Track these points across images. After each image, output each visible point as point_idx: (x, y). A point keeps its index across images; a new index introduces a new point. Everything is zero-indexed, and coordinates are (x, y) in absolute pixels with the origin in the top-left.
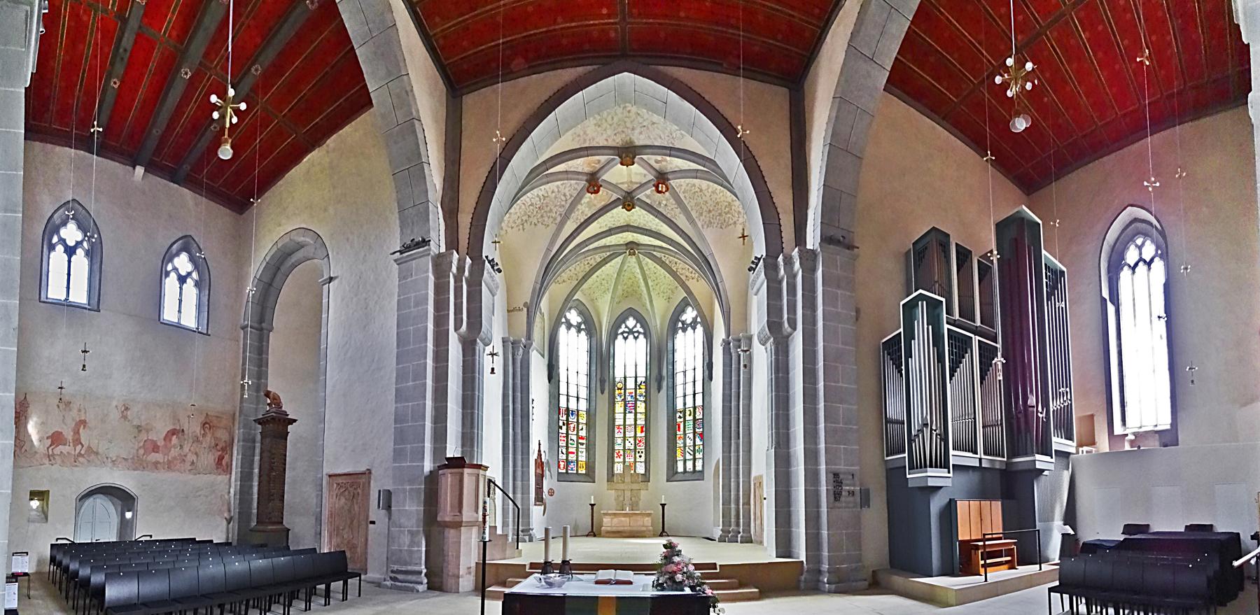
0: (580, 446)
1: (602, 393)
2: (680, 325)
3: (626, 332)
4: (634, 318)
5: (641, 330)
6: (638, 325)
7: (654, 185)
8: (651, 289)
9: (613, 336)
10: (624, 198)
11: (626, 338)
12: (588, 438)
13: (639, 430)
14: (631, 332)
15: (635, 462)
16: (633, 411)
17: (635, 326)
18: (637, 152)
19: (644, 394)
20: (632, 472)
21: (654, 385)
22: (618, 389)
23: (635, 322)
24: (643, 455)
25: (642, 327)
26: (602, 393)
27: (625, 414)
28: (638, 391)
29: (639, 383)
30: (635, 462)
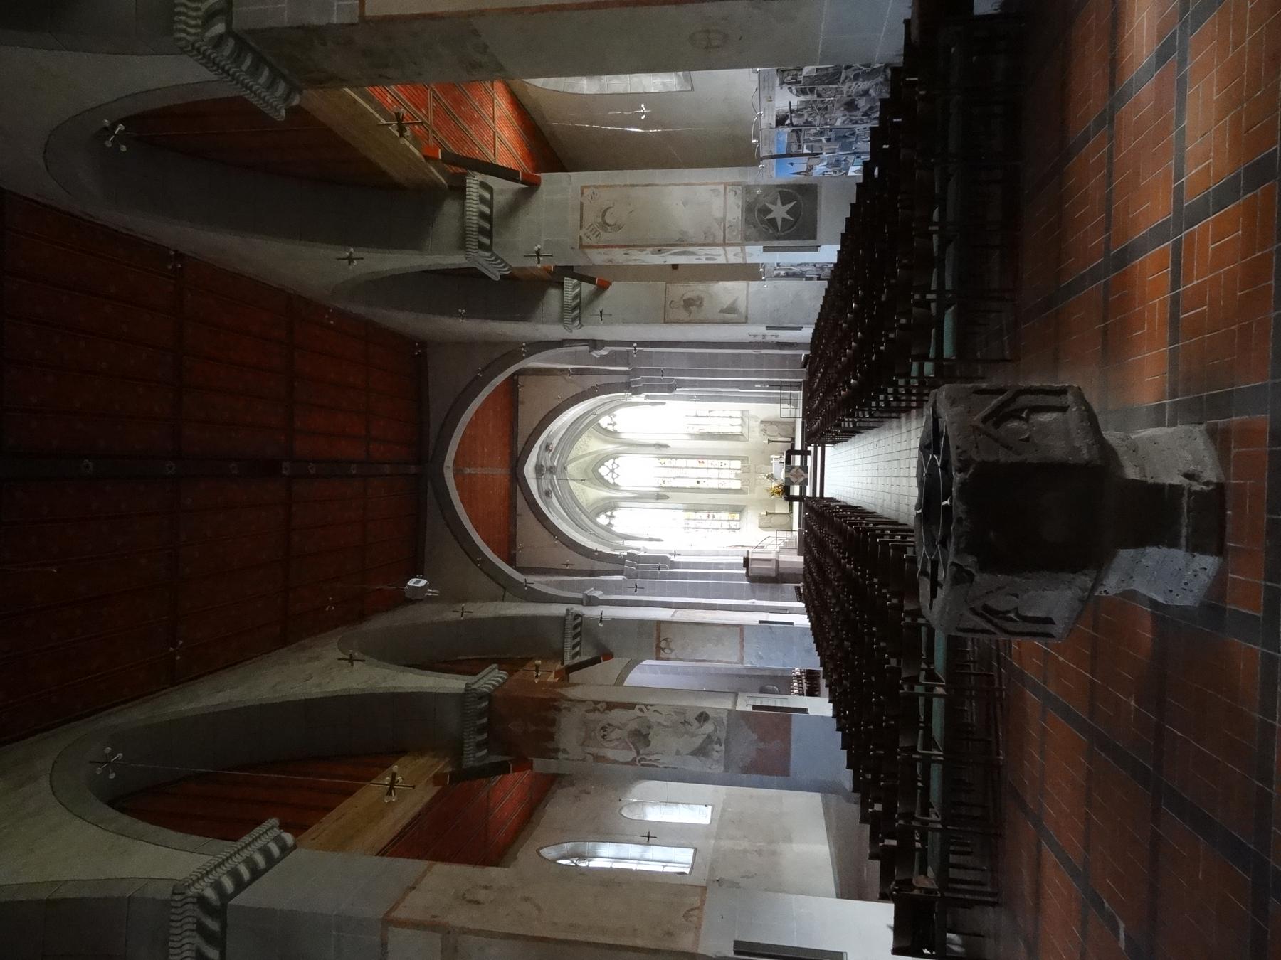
0: (715, 518)
1: (668, 498)
2: (610, 428)
5: (612, 461)
6: (606, 464)
8: (584, 453)
9: (615, 487)
12: (709, 511)
14: (612, 471)
15: (730, 469)
16: (685, 469)
17: (607, 467)
18: (539, 464)
19: (669, 459)
20: (739, 472)
21: (664, 451)
23: (603, 467)
24: (724, 461)
26: (668, 498)
27: (686, 477)
28: (667, 465)
29: (660, 465)
30: (730, 469)
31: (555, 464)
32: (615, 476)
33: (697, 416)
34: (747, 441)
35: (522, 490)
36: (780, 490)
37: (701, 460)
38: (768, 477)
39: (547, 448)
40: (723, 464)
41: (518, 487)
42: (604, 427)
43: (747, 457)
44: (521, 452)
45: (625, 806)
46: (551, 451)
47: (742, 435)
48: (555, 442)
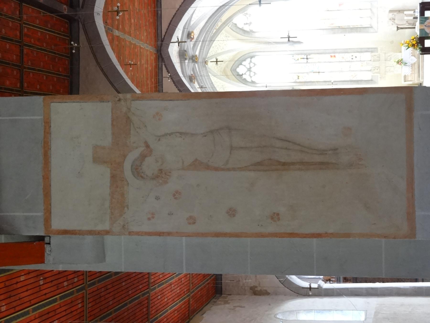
3: (250, 73)
4: (238, 67)
5: (248, 60)
6: (244, 63)
7: (191, 41)
8: (223, 51)
10: (193, 62)
11: (255, 73)
13: (333, 59)
14: (249, 70)
17: (245, 66)
18: (182, 49)
22: (298, 78)
23: (240, 66)
25: (245, 60)
31: (197, 53)
32: (252, 74)
33: (328, 10)
34: (376, 32)
35: (167, 69)
36: (414, 43)
37: (333, 55)
38: (398, 62)
39: (189, 35)
40: (354, 57)
41: (164, 66)
42: (241, 27)
43: (376, 48)
44: (166, 33)
45: (279, 313)
46: (193, 39)
47: (372, 27)
48: (196, 33)
